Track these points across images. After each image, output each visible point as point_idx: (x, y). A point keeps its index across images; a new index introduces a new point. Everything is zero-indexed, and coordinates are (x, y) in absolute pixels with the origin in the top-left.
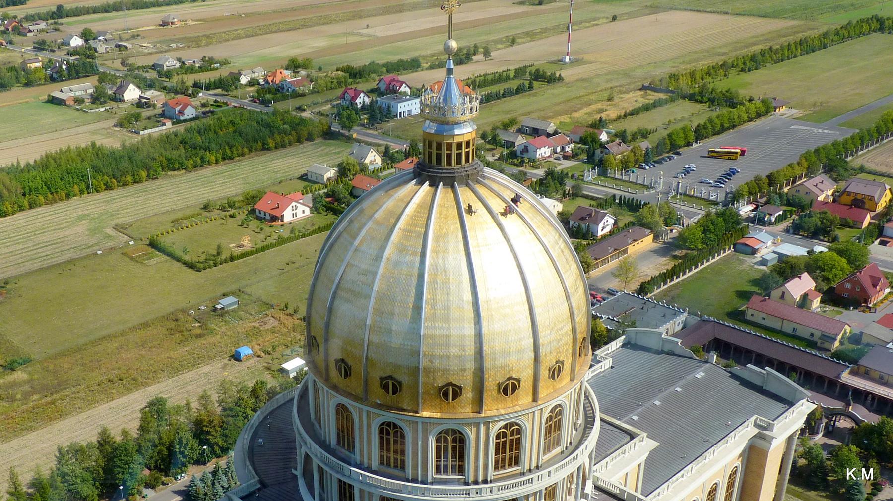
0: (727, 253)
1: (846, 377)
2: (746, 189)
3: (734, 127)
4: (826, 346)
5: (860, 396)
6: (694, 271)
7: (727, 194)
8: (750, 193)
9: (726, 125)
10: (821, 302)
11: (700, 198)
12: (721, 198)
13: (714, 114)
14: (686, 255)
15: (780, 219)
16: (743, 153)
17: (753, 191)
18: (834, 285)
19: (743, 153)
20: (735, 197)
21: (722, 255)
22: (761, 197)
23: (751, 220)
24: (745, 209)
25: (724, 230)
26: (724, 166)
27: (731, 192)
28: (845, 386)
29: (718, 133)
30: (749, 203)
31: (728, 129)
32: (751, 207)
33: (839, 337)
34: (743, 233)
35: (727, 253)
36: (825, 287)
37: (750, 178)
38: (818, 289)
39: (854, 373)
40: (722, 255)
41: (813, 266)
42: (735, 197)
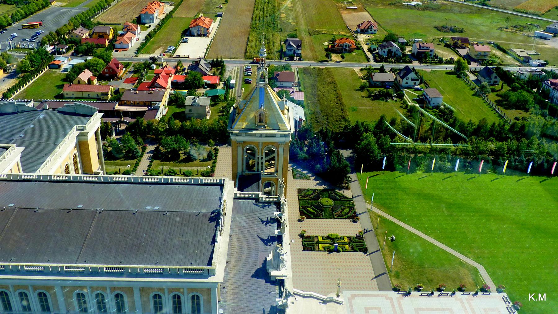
0: (46, 70)
1: (117, 108)
2: (47, 39)
3: (32, 14)
4: (105, 98)
5: (126, 113)
6: (31, 82)
7: (37, 43)
8: (49, 41)
9: (28, 13)
10: (97, 81)
11: (24, 48)
12: (35, 46)
13: (19, 9)
14: (23, 76)
15: (68, 50)
16: (40, 24)
17: (50, 39)
18: (101, 72)
19: (40, 24)
20: (42, 43)
21: (44, 72)
22: (56, 42)
23: (53, 53)
24: (49, 49)
25: (40, 61)
26: (33, 32)
27: (39, 42)
28: (118, 112)
29: (25, 17)
30: (50, 45)
31: (29, 15)
32: (52, 47)
33: (110, 93)
34: (51, 59)
35: (46, 70)
36: (97, 74)
37: (47, 34)
38: (94, 75)
39: (119, 105)
40: (44, 72)
41: (88, 66)
42: (42, 43)
